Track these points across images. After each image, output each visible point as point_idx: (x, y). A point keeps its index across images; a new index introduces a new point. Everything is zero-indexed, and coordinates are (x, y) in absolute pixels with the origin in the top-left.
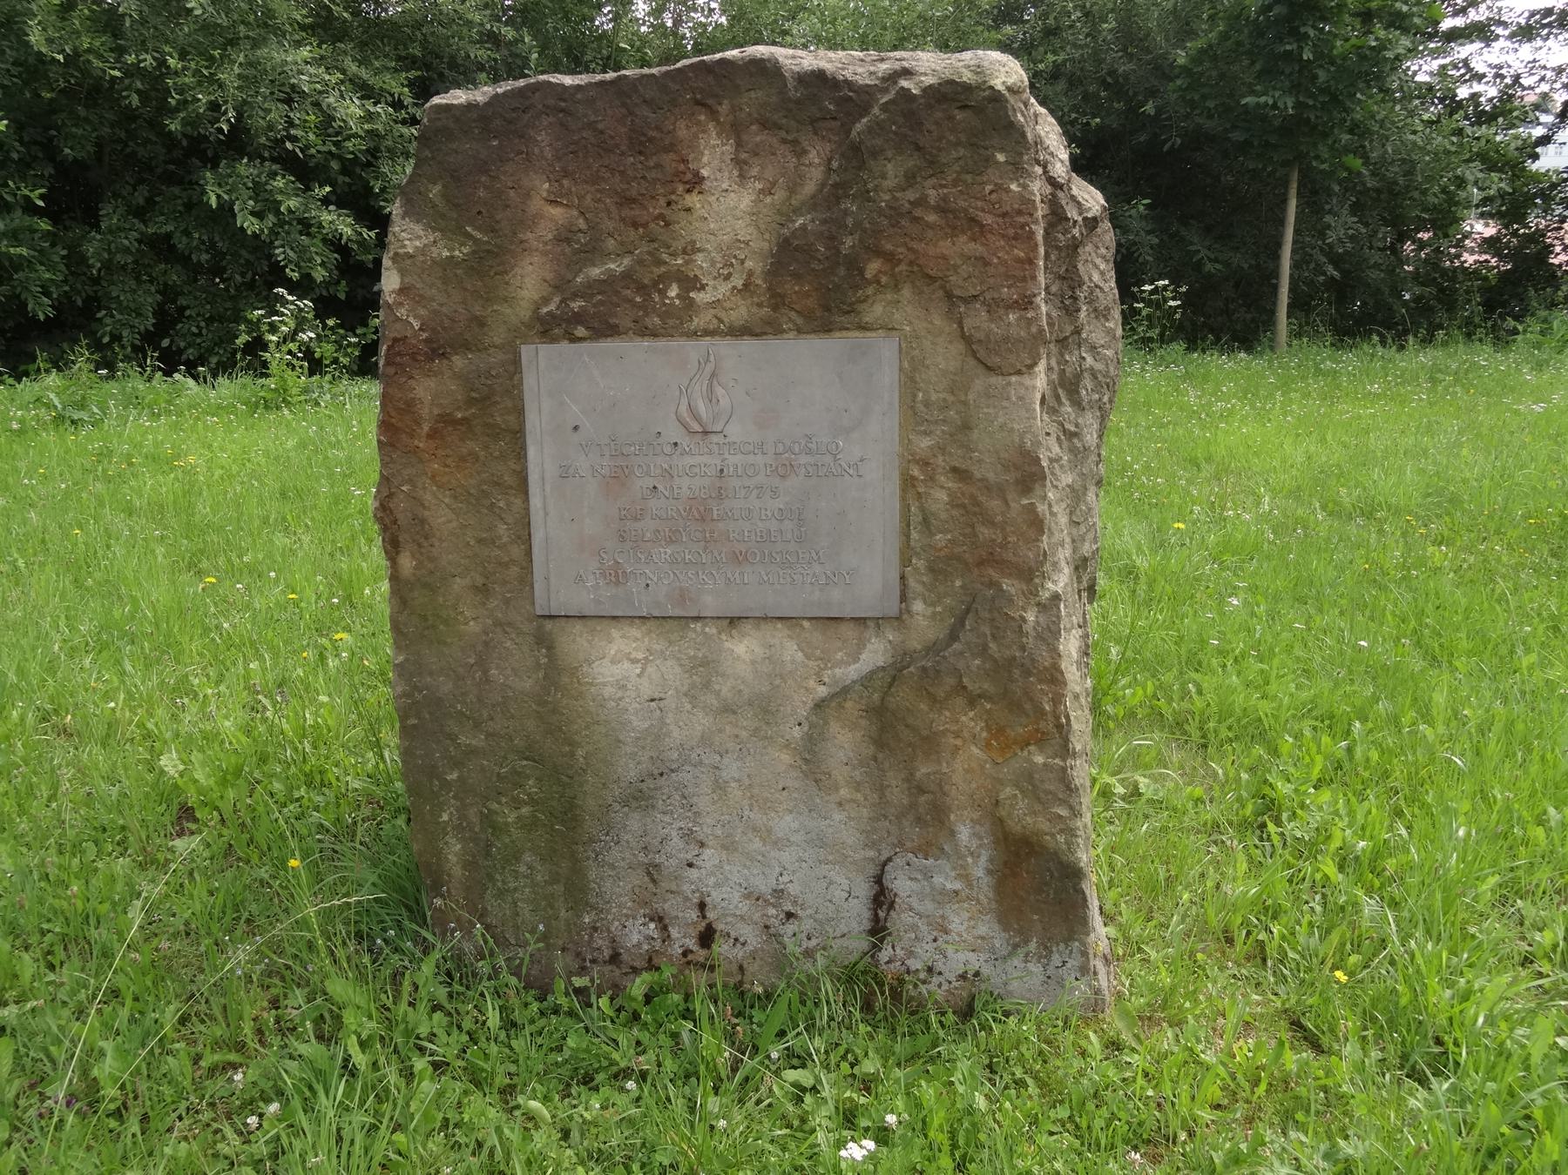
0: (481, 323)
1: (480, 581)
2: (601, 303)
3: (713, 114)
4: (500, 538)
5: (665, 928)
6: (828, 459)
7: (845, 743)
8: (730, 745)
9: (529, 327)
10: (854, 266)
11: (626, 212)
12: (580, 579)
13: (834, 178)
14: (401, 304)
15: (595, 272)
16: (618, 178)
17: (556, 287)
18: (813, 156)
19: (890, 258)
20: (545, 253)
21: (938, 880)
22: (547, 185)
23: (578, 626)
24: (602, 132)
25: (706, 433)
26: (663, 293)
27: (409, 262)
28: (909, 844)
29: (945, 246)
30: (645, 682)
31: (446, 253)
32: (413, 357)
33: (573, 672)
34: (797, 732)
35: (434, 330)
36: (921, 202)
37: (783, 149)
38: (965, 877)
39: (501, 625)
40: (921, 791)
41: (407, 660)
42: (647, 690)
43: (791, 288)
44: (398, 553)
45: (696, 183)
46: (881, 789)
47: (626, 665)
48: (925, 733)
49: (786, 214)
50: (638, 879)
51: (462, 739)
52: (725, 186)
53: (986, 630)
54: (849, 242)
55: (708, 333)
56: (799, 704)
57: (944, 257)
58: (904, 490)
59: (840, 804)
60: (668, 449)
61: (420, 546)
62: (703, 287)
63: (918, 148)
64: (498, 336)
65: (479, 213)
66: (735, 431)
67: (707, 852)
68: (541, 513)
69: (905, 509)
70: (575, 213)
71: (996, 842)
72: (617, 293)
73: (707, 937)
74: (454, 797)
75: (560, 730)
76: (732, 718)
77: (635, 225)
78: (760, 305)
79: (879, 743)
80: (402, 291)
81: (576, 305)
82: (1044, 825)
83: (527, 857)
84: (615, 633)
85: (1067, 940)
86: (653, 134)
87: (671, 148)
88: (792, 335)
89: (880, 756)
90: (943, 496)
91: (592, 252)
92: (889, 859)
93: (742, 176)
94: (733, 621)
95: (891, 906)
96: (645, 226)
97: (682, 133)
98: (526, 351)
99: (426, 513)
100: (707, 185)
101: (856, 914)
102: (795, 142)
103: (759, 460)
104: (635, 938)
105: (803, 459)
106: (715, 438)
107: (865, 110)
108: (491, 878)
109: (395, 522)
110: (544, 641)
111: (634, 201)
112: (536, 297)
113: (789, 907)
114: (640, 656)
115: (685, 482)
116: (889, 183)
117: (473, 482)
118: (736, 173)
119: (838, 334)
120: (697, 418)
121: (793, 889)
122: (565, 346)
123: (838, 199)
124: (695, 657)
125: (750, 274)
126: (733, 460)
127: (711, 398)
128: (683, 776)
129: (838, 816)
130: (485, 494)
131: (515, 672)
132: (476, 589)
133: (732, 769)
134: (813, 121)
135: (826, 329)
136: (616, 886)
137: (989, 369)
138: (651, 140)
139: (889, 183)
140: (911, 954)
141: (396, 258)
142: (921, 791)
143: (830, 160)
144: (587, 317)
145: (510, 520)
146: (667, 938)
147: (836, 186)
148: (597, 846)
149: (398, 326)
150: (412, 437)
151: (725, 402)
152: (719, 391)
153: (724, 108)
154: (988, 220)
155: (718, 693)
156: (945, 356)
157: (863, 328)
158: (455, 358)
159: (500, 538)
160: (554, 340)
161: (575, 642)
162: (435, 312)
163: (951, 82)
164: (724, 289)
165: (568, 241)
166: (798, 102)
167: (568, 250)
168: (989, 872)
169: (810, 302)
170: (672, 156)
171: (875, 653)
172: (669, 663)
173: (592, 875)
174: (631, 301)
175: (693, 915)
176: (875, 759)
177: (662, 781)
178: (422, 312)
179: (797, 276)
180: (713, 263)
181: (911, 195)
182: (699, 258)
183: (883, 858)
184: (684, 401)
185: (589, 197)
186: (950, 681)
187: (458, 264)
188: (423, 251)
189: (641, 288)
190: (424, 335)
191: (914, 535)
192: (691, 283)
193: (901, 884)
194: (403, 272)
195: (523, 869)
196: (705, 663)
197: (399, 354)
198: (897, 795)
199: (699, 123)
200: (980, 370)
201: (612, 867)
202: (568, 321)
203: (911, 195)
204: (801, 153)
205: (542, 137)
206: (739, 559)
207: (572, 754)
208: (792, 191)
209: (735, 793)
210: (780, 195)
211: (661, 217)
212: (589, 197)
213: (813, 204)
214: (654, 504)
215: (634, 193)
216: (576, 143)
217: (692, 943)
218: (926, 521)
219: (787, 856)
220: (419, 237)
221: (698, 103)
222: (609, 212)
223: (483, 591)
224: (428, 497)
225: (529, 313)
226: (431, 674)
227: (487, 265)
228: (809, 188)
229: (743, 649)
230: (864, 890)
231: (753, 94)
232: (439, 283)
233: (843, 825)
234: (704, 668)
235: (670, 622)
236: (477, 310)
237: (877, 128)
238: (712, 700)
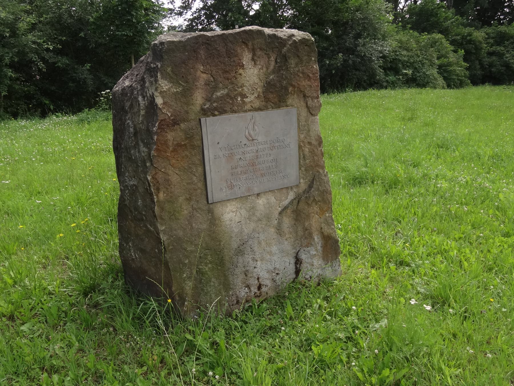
0: (187, 112)
1: (188, 197)
2: (221, 103)
3: (247, 45)
4: (194, 181)
5: (250, 288)
6: (282, 143)
7: (287, 222)
8: (261, 230)
9: (199, 112)
10: (286, 89)
11: (225, 75)
12: (221, 189)
13: (278, 65)
14: (164, 108)
15: (219, 94)
16: (223, 65)
17: (206, 99)
18: (272, 59)
19: (294, 86)
20: (202, 89)
21: (311, 252)
22: (202, 67)
23: (219, 204)
24: (219, 51)
25: (253, 140)
26: (237, 100)
27: (165, 94)
28: (304, 245)
29: (304, 83)
30: (237, 217)
31: (175, 90)
32: (168, 126)
33: (219, 219)
34: (276, 222)
35: (175, 116)
36: (298, 71)
37: (265, 56)
38: (316, 250)
39: (196, 209)
40: (306, 230)
41: (166, 228)
42: (237, 220)
43: (271, 96)
44: (159, 193)
45: (242, 66)
46: (296, 232)
47: (231, 213)
48: (307, 214)
49: (267, 75)
50: (242, 276)
51: (188, 249)
52: (250, 67)
53: (318, 183)
54: (285, 82)
55: (250, 110)
56: (276, 214)
57: (304, 86)
58: (299, 150)
59: (286, 239)
60: (243, 146)
61: (167, 189)
62: (247, 97)
63: (298, 56)
64: (192, 116)
65: (183, 76)
66: (260, 139)
67: (258, 262)
68: (209, 171)
69: (300, 155)
70: (210, 76)
71: (322, 239)
72: (225, 100)
73: (259, 288)
74: (188, 268)
75: (216, 238)
76: (260, 222)
77: (228, 79)
78: (262, 101)
79: (296, 220)
80: (165, 103)
81: (215, 105)
82: (331, 232)
83: (213, 280)
84: (228, 204)
85: (336, 259)
86: (232, 51)
87: (236, 56)
88: (271, 109)
89: (296, 223)
90: (307, 150)
91: (215, 88)
92: (299, 251)
93: (255, 64)
94: (258, 195)
95: (301, 263)
96: (231, 79)
97: (239, 51)
98: (203, 120)
99: (170, 177)
100: (245, 67)
101: (292, 268)
102: (268, 54)
103: (266, 146)
104: (243, 294)
105: (277, 144)
106: (255, 141)
107: (285, 46)
108: (202, 290)
109: (158, 182)
110: (210, 211)
111: (227, 72)
112: (201, 103)
113: (277, 272)
114: (235, 210)
115: (248, 155)
116: (293, 66)
117: (186, 164)
118: (253, 63)
119: (281, 108)
120: (251, 136)
121: (278, 267)
122: (211, 118)
123: (280, 70)
124: (250, 207)
125: (259, 92)
126: (260, 147)
127: (254, 129)
128: (250, 242)
129: (286, 243)
130: (190, 168)
131: (201, 223)
132: (187, 199)
133: (262, 237)
134: (273, 48)
135: (279, 107)
136: (238, 280)
137: (312, 114)
138: (232, 53)
139: (293, 66)
140: (307, 274)
141: (161, 93)
142: (306, 230)
143: (276, 59)
144: (217, 108)
145: (197, 175)
146: (250, 291)
147: (279, 67)
148: (231, 270)
149: (163, 115)
150: (166, 152)
151: (257, 130)
152: (256, 127)
153: (250, 44)
154: (311, 75)
155: (256, 216)
156: (304, 112)
157: (287, 106)
158: (181, 124)
159: (194, 181)
160: (208, 116)
161: (219, 210)
162: (174, 110)
163: (304, 39)
164: (253, 97)
165: (209, 85)
166: (269, 43)
167: (209, 88)
168: (321, 247)
169: (276, 100)
170: (237, 58)
171: (291, 196)
172: (243, 210)
173: (231, 279)
174: (229, 102)
175: (257, 282)
176: (295, 224)
177: (245, 245)
178: (171, 110)
179: (272, 92)
180: (248, 89)
181: (297, 69)
182: (244, 88)
183: (298, 250)
184: (247, 131)
185: (214, 71)
186: (312, 199)
187: (179, 93)
188: (169, 89)
189: (231, 98)
190: (172, 118)
191: (301, 161)
192: (244, 96)
193: (303, 256)
194: (163, 97)
195: (212, 284)
196: (253, 208)
197: (163, 125)
198: (300, 233)
199: (243, 48)
200: (310, 115)
201: (236, 275)
202: (213, 110)
203: (297, 69)
204: (269, 58)
205: (202, 52)
206: (262, 175)
207: (220, 244)
208: (267, 68)
209: (263, 243)
210: (265, 69)
211: (234, 76)
212: (214, 71)
213: (273, 72)
214: (241, 163)
215: (228, 69)
216: (211, 54)
217: (256, 290)
218: (304, 157)
219: (275, 258)
220: (167, 85)
221: (244, 42)
222: (220, 76)
223: (189, 200)
224: (170, 172)
225: (199, 108)
226: (175, 230)
227: (186, 94)
228: (272, 67)
229: (261, 202)
230: (293, 261)
231: (258, 40)
232: (174, 100)
233: (287, 246)
234: (252, 209)
235: (243, 198)
236: (186, 108)
237: (289, 50)
238: (255, 218)
